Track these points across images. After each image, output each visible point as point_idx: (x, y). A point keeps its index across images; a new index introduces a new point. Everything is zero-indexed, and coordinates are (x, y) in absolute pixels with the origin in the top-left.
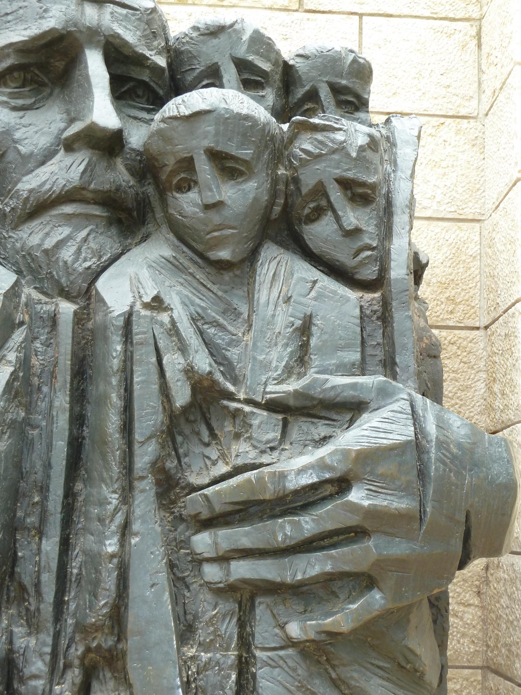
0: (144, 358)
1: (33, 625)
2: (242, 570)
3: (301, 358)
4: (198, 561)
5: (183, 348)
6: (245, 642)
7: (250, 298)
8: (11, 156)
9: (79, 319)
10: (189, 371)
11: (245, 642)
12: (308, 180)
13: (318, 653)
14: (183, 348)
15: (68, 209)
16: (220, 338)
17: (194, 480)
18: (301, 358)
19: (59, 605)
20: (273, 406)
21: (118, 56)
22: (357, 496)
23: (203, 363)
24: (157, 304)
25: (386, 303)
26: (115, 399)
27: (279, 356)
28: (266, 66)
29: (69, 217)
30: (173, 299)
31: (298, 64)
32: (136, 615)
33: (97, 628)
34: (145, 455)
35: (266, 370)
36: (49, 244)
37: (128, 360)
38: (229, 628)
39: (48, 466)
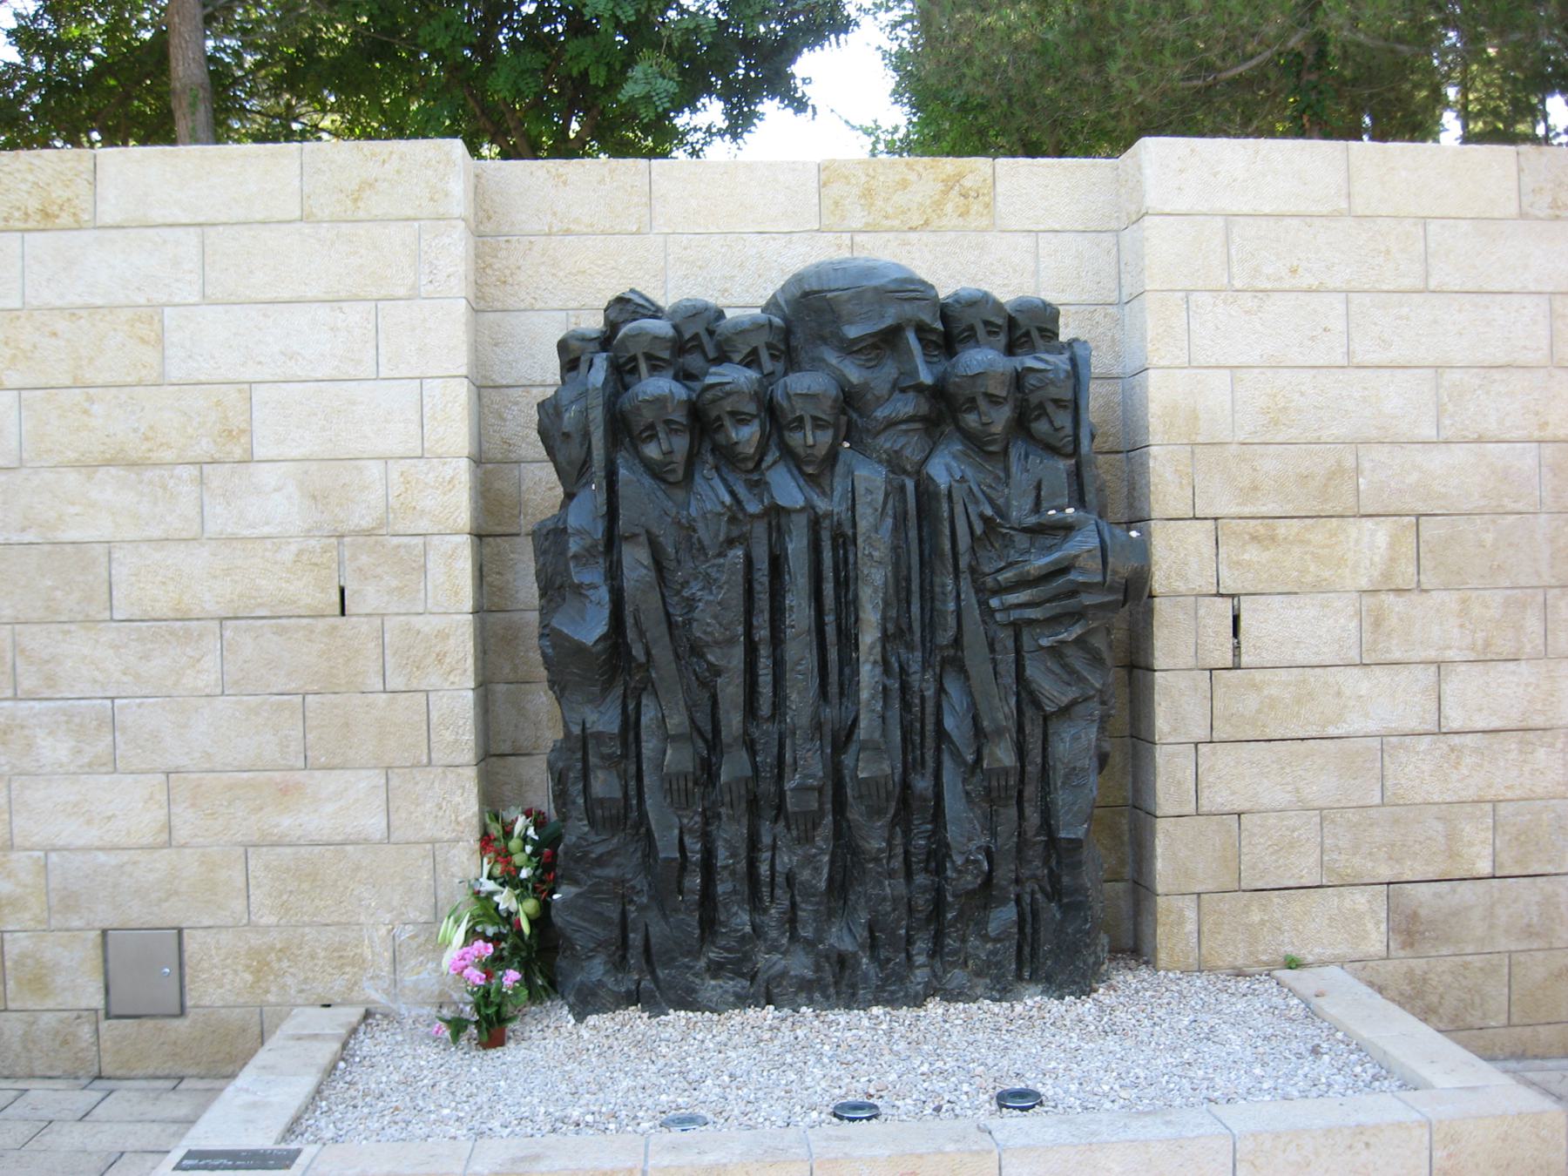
0: (959, 509)
1: (910, 647)
2: (1015, 615)
3: (1037, 507)
4: (992, 611)
5: (977, 502)
6: (1018, 651)
7: (1007, 470)
8: (869, 396)
9: (917, 487)
10: (982, 516)
11: (1018, 651)
12: (1034, 399)
13: (1056, 651)
14: (977, 502)
15: (904, 427)
16: (993, 495)
17: (987, 570)
18: (1037, 507)
19: (923, 637)
20: (1025, 530)
21: (921, 329)
22: (1074, 576)
23: (989, 512)
24: (963, 479)
25: (1078, 466)
26: (947, 532)
27: (1028, 503)
28: (1000, 321)
29: (906, 432)
30: (969, 473)
31: (1020, 318)
32: (967, 639)
33: (947, 647)
34: (964, 562)
35: (1020, 510)
36: (897, 447)
37: (952, 510)
38: (1010, 644)
39: (909, 568)
